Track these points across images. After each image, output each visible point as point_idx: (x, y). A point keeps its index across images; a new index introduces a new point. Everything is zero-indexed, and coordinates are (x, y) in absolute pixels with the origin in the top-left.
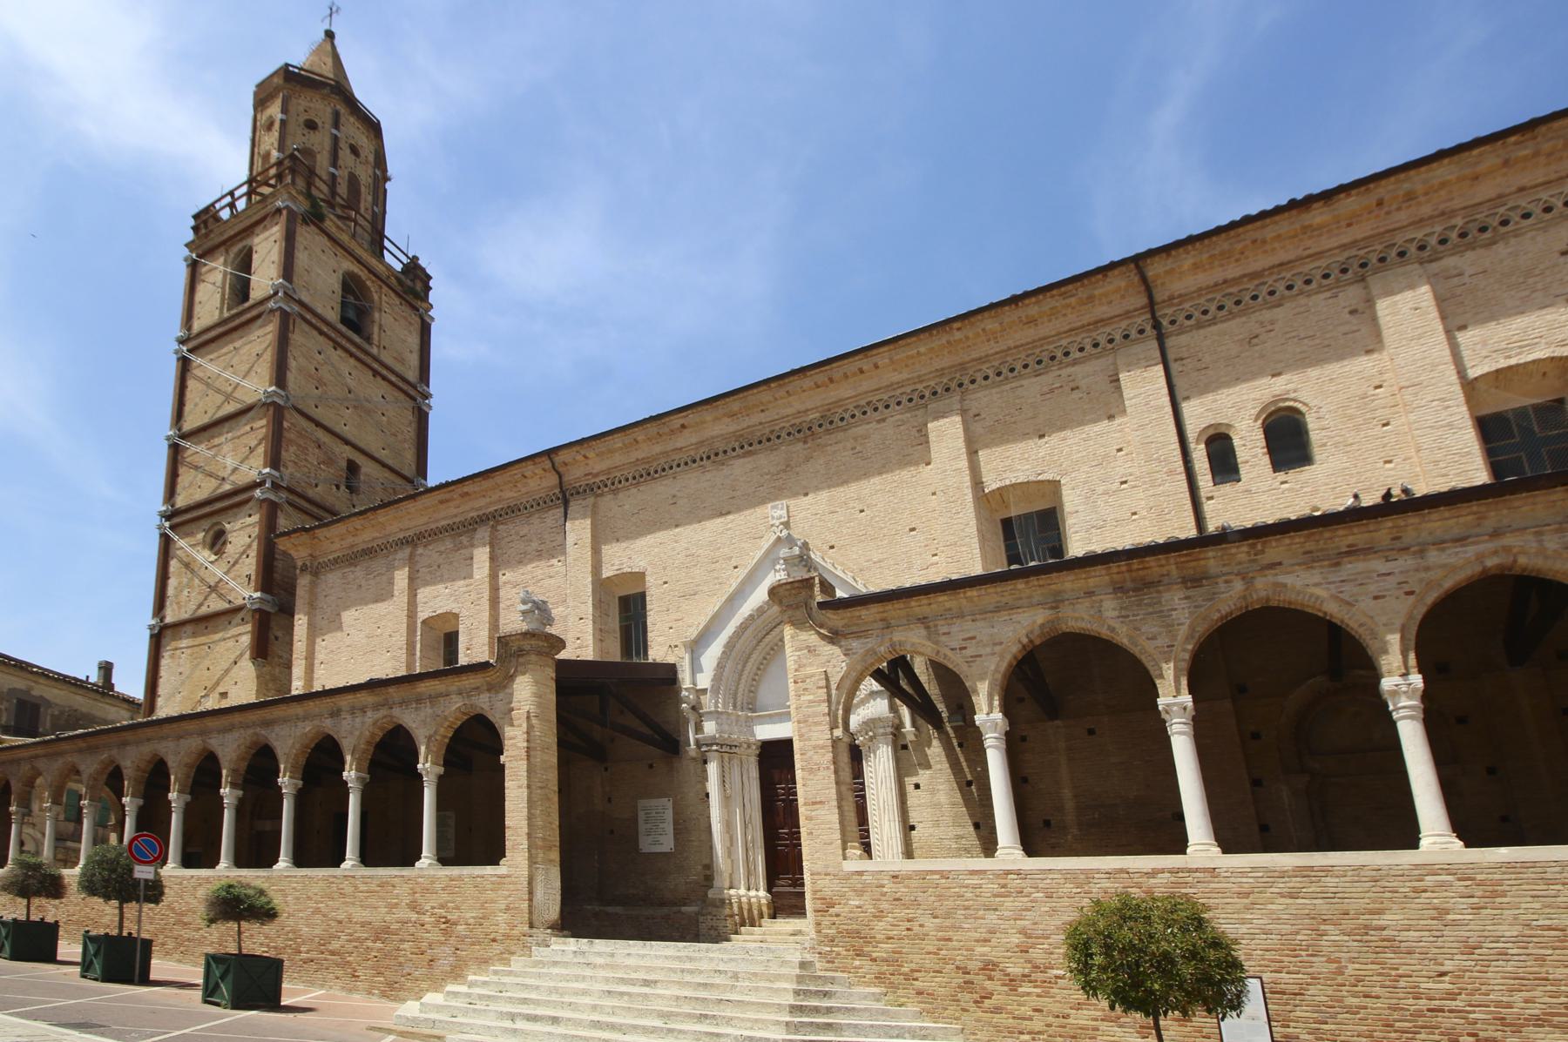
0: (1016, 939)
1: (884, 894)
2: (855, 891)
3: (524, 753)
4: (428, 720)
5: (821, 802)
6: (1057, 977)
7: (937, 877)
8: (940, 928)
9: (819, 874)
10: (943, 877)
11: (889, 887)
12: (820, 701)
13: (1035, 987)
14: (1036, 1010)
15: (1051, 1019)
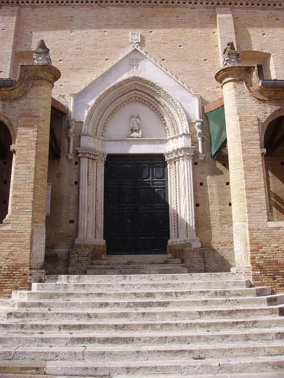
2: (275, 238)
3: (34, 145)
9: (254, 230)
12: (255, 133)
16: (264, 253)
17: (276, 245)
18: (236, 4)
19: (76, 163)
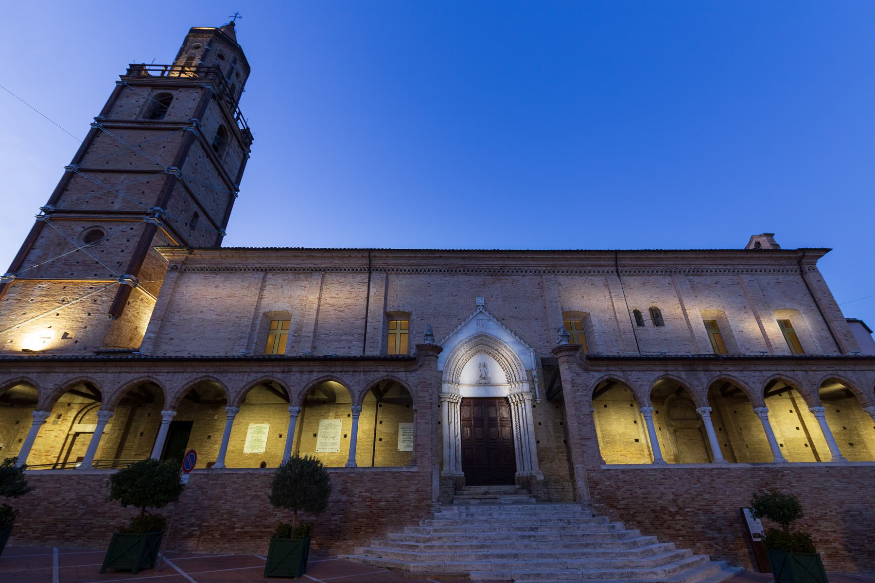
0: (671, 497)
1: (619, 479)
4: (361, 382)
5: (588, 439)
6: (688, 512)
7: (639, 471)
8: (643, 494)
9: (591, 470)
10: (642, 472)
11: (621, 476)
13: (681, 516)
14: (682, 526)
15: (689, 530)
16: (600, 489)
17: (608, 483)
18: (558, 272)
19: (439, 406)
